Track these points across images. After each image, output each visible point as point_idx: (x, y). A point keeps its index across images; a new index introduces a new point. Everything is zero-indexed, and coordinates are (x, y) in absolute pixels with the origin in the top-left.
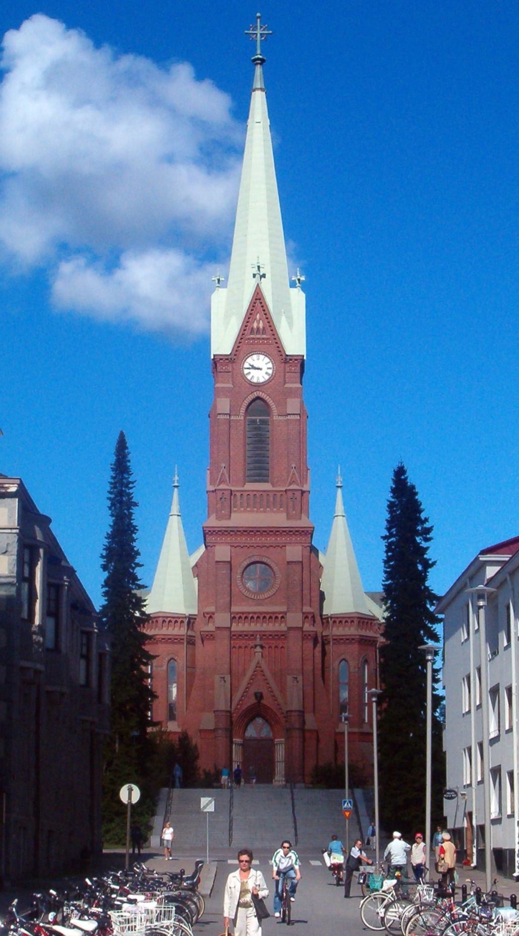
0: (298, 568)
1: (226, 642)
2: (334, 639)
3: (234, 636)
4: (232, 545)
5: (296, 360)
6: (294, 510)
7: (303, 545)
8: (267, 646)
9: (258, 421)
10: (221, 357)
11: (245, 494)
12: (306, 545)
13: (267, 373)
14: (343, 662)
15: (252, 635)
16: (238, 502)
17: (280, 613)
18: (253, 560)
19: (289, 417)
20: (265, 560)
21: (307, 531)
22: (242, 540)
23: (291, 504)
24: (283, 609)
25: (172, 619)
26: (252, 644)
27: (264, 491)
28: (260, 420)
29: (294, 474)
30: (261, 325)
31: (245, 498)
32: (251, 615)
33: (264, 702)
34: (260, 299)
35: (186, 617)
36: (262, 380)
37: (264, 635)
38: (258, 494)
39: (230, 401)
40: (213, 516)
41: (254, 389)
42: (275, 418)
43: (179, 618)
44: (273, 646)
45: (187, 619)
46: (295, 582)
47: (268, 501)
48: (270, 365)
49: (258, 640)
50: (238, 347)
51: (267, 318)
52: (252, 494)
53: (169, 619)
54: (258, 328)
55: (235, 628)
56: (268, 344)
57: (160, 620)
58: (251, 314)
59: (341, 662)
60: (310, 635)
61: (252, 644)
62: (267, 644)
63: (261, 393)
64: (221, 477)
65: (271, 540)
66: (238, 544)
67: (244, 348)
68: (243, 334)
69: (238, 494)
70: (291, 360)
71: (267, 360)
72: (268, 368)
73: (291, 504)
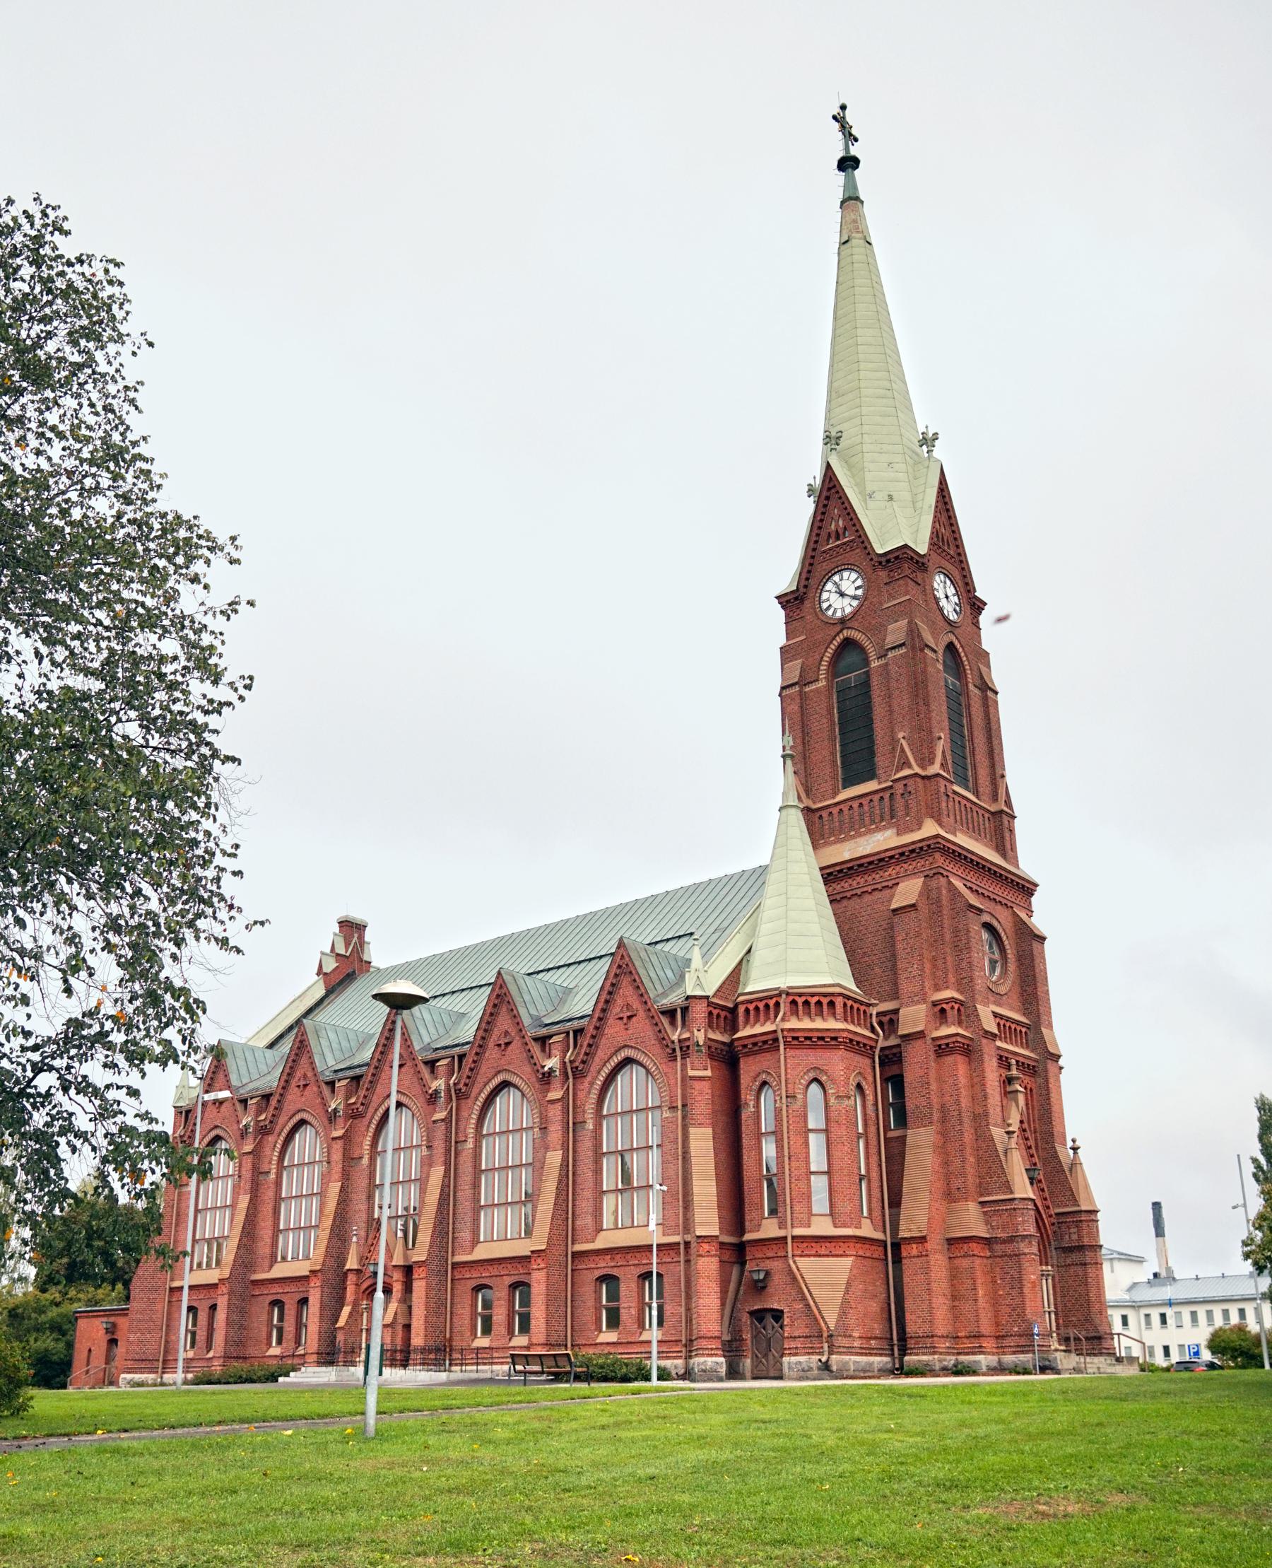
19: (890, 655)
36: (848, 610)
38: (855, 804)
67: (820, 569)
69: (825, 814)
70: (888, 561)
71: (854, 575)
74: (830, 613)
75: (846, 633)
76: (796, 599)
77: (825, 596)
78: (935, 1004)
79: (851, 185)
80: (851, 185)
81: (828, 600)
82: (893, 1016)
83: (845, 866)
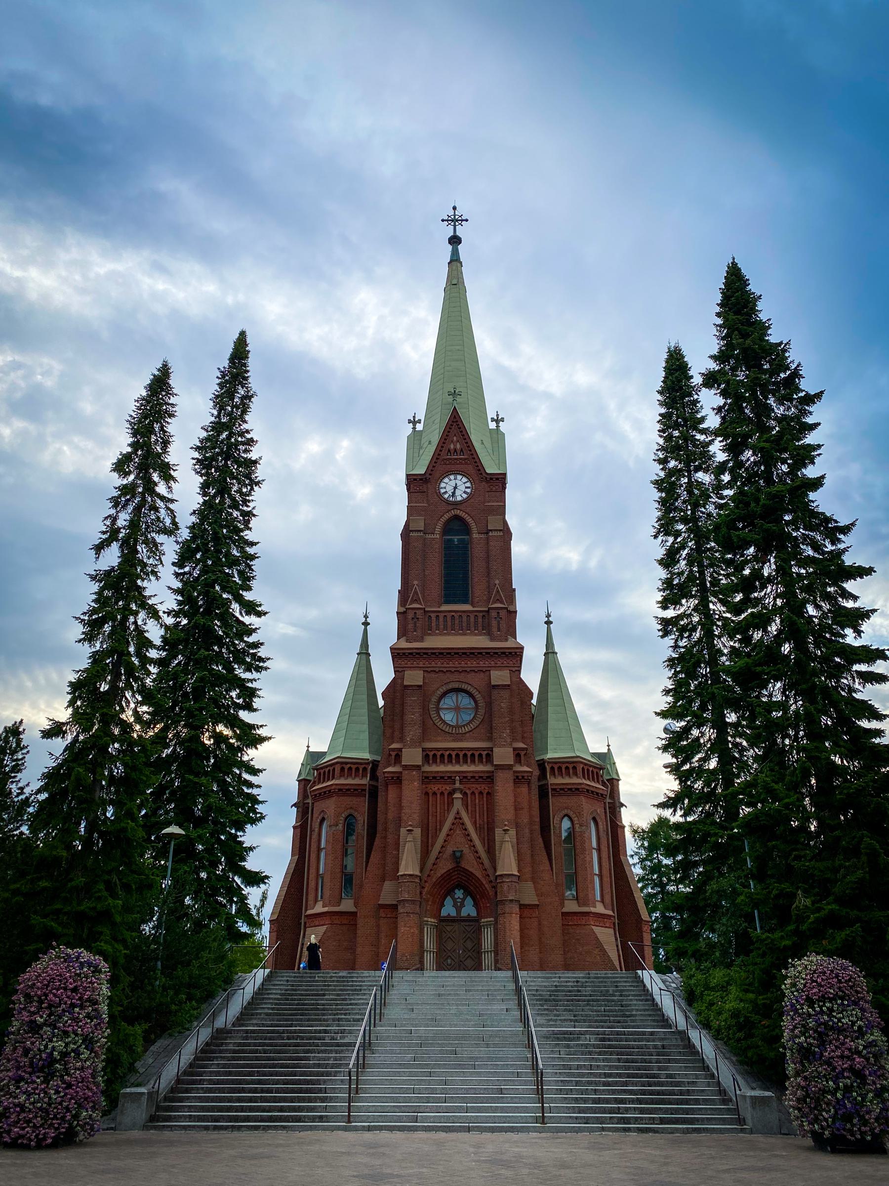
3: (427, 779)
6: (499, 631)
8: (468, 792)
9: (456, 540)
10: (415, 477)
11: (441, 615)
12: (514, 669)
13: (465, 492)
14: (566, 819)
15: (450, 777)
16: (434, 624)
17: (484, 749)
18: (451, 686)
20: (465, 686)
21: (516, 653)
22: (438, 664)
25: (352, 766)
26: (449, 788)
27: (464, 612)
28: (458, 539)
29: (498, 591)
30: (458, 446)
31: (441, 619)
32: (448, 753)
33: (464, 864)
34: (457, 421)
35: (368, 764)
37: (465, 778)
39: (425, 520)
41: (450, 507)
42: (475, 536)
43: (361, 764)
47: (468, 624)
48: (468, 484)
49: (457, 785)
50: (434, 467)
52: (449, 615)
53: (349, 766)
54: (455, 450)
55: (427, 768)
56: (466, 464)
57: (338, 768)
58: (447, 436)
59: (563, 818)
60: (523, 777)
61: (449, 788)
62: (469, 789)
65: (472, 664)
66: (432, 669)
69: (433, 615)
71: (465, 480)
72: (467, 488)
73: (494, 623)
75: (458, 512)
76: (421, 479)
77: (443, 485)
78: (515, 749)
82: (490, 753)
83: (430, 651)
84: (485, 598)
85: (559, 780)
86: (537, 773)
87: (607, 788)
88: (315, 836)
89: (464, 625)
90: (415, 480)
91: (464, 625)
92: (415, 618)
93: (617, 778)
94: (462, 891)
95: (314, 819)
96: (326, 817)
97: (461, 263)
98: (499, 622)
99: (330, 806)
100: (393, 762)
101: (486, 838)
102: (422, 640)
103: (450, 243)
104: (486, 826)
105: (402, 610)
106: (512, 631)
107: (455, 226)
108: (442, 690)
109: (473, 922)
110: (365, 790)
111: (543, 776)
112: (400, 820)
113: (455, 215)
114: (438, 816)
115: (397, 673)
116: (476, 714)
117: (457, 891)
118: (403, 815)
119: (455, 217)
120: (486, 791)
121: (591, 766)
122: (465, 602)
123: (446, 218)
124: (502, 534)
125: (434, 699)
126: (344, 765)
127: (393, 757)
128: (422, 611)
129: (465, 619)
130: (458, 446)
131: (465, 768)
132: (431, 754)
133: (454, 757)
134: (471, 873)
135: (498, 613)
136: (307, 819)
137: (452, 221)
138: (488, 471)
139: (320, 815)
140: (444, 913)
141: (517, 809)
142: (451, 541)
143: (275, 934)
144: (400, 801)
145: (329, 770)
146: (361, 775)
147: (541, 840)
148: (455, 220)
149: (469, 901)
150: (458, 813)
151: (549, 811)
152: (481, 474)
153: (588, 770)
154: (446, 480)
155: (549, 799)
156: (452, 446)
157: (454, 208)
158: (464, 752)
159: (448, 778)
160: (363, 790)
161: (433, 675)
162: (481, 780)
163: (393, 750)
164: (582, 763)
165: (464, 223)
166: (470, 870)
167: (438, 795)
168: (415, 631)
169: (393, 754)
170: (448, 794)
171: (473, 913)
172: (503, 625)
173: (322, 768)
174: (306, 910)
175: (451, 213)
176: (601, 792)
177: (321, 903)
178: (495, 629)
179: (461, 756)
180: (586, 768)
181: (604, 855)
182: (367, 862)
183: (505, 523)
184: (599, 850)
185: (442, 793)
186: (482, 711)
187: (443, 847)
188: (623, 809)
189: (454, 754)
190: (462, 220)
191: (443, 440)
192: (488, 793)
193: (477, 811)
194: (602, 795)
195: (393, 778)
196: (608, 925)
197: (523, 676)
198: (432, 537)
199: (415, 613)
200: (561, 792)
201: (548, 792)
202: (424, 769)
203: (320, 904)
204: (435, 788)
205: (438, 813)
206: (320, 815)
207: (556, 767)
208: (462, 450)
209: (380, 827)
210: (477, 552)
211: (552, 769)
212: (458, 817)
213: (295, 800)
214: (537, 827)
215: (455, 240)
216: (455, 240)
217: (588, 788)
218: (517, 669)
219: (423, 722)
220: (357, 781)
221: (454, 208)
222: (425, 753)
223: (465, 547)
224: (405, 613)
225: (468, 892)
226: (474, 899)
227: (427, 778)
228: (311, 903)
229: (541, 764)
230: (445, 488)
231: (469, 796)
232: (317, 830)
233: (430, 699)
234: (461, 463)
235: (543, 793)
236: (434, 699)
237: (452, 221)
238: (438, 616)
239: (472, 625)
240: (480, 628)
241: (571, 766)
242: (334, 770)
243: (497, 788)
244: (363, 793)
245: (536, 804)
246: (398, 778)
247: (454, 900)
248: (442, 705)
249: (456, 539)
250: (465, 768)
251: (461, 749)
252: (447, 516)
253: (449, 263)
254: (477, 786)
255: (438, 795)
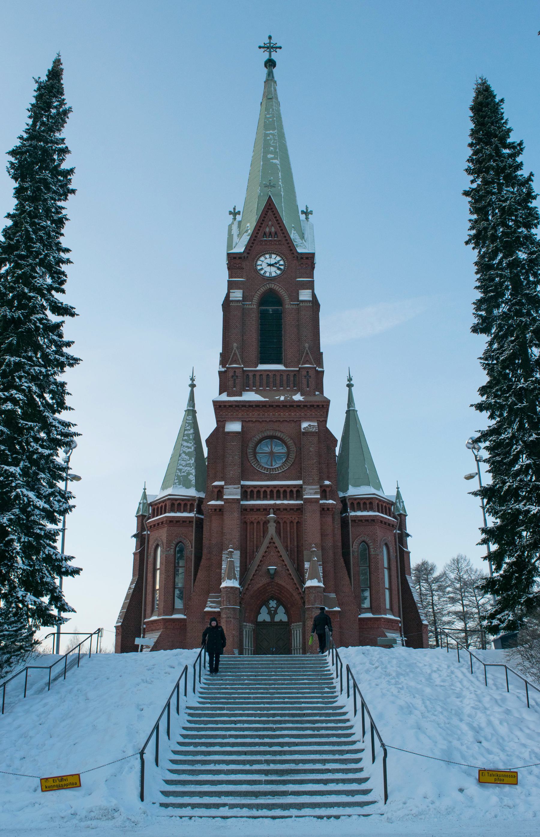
0: (315, 439)
1: (236, 515)
2: (354, 521)
3: (245, 510)
4: (243, 419)
5: (307, 258)
7: (319, 419)
9: (270, 310)
12: (321, 420)
15: (265, 510)
16: (251, 382)
17: (295, 486)
20: (278, 434)
21: (323, 406)
22: (254, 415)
23: (304, 381)
24: (300, 482)
28: (273, 310)
29: (307, 353)
30: (273, 230)
32: (263, 489)
34: (272, 209)
35: (194, 500)
36: (274, 274)
37: (277, 509)
40: (225, 394)
42: (287, 306)
44: (288, 522)
45: (197, 502)
46: (311, 453)
47: (281, 381)
51: (279, 224)
53: (178, 502)
54: (270, 233)
57: (168, 503)
63: (273, 285)
64: (233, 356)
68: (256, 237)
69: (251, 375)
73: (304, 381)
74: (262, 272)
76: (240, 258)
77: (259, 263)
79: (270, 75)
80: (270, 75)
81: (261, 265)
82: (300, 489)
84: (296, 360)
85: (359, 513)
86: (340, 506)
87: (397, 520)
88: (151, 559)
89: (278, 382)
90: (235, 258)
91: (278, 382)
92: (234, 376)
93: (405, 514)
94: (275, 602)
95: (150, 546)
96: (160, 543)
97: (275, 82)
98: (308, 380)
99: (163, 534)
100: (216, 496)
101: (296, 559)
102: (241, 395)
103: (266, 66)
104: (296, 549)
105: (223, 370)
106: (320, 387)
107: (270, 53)
108: (260, 436)
109: (285, 626)
110: (192, 522)
111: (344, 510)
112: (222, 545)
113: (270, 43)
114: (255, 542)
115: (219, 423)
116: (288, 457)
117: (271, 602)
118: (225, 540)
119: (270, 45)
120: (296, 521)
121: (384, 502)
122: (279, 362)
123: (263, 45)
124: (311, 305)
125: (251, 445)
126: (174, 502)
127: (216, 493)
128: (241, 370)
129: (278, 378)
130: (273, 230)
131: (278, 502)
132: (249, 490)
133: (268, 492)
134: (284, 587)
135: (308, 372)
136: (144, 547)
137: (268, 48)
138: (300, 250)
139: (154, 542)
140: (260, 618)
141: (323, 535)
142: (268, 310)
143: (120, 637)
144: (222, 529)
145: (162, 506)
146: (188, 510)
147: (342, 560)
148: (270, 47)
149: (281, 609)
150: (272, 539)
151: (349, 539)
152: (293, 253)
153: (382, 505)
154: (262, 258)
155: (348, 528)
156: (267, 230)
157: (270, 38)
158: (277, 489)
159: (266, 510)
160: (190, 522)
161: (250, 424)
162: (292, 512)
163: (216, 487)
164: (377, 499)
165: (278, 50)
166: (283, 584)
167: (255, 525)
168: (235, 387)
169: (216, 490)
170: (263, 524)
171: (285, 619)
172: (312, 382)
173: (156, 504)
174: (145, 618)
175: (267, 41)
176: (392, 523)
177: (157, 613)
178: (305, 386)
179: (275, 492)
180: (380, 503)
181: (394, 573)
182: (195, 580)
183: (314, 296)
184: (389, 569)
185: (258, 523)
186: (293, 456)
187: (259, 566)
188: (409, 539)
189: (268, 490)
190: (276, 48)
191: (259, 224)
192: (298, 523)
193: (289, 537)
194: (393, 526)
195: (215, 510)
196: (395, 628)
197: (329, 426)
198: (250, 307)
199: (235, 372)
200: (360, 523)
201: (348, 523)
202: (242, 503)
203: (156, 612)
204: (253, 517)
205: (255, 539)
206: (154, 542)
207: (355, 503)
208: (276, 233)
209: (205, 551)
210: (289, 321)
211: (352, 504)
212: (272, 542)
213: (135, 532)
214: (340, 551)
215: (270, 64)
216: (270, 64)
217: (382, 519)
218: (323, 419)
219: (242, 464)
220: (185, 514)
221: (270, 38)
222: (244, 490)
223: (278, 317)
224: (225, 371)
225: (280, 602)
226: (285, 608)
227: (246, 510)
228: (149, 611)
229: (343, 500)
230: (261, 265)
231: (282, 525)
232: (152, 554)
233: (248, 445)
234: (276, 244)
235: (345, 523)
236: (251, 445)
237: (268, 48)
238: (255, 375)
239: (285, 382)
240: (292, 385)
241: (368, 502)
242: (166, 505)
243: (306, 517)
244: (191, 524)
245: (338, 532)
246: (220, 510)
247: (269, 608)
248: (258, 450)
249: (270, 309)
250: (278, 502)
251: (275, 486)
252: (262, 290)
253: (265, 82)
254: (288, 516)
255: (255, 525)
